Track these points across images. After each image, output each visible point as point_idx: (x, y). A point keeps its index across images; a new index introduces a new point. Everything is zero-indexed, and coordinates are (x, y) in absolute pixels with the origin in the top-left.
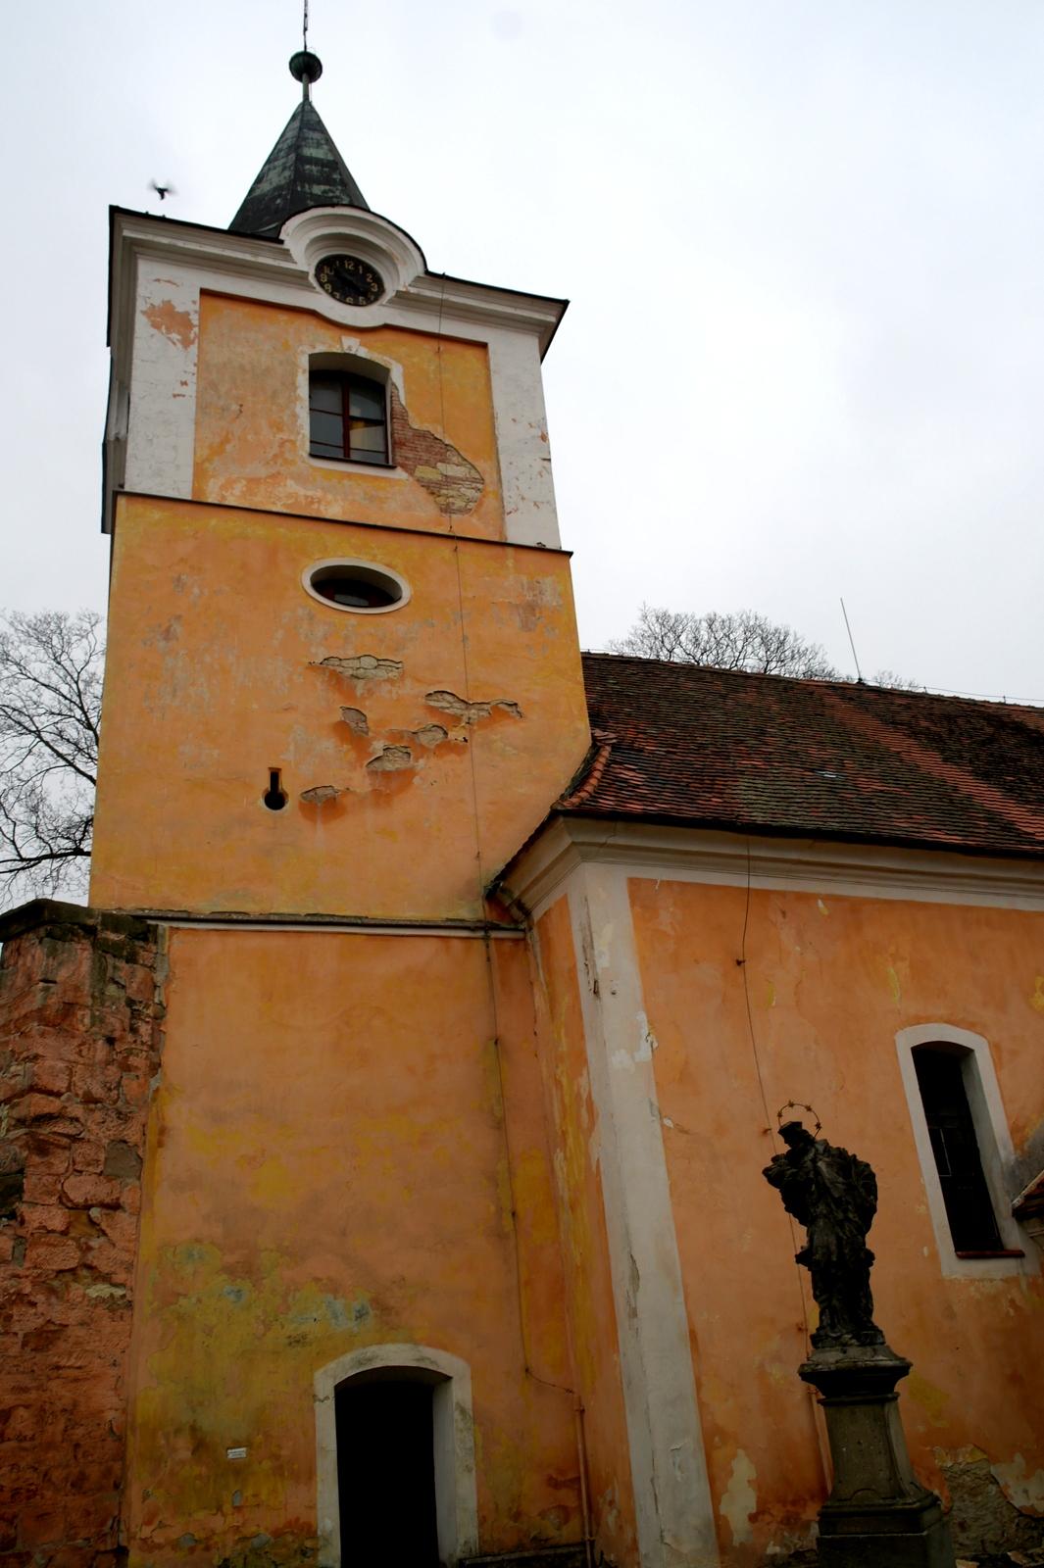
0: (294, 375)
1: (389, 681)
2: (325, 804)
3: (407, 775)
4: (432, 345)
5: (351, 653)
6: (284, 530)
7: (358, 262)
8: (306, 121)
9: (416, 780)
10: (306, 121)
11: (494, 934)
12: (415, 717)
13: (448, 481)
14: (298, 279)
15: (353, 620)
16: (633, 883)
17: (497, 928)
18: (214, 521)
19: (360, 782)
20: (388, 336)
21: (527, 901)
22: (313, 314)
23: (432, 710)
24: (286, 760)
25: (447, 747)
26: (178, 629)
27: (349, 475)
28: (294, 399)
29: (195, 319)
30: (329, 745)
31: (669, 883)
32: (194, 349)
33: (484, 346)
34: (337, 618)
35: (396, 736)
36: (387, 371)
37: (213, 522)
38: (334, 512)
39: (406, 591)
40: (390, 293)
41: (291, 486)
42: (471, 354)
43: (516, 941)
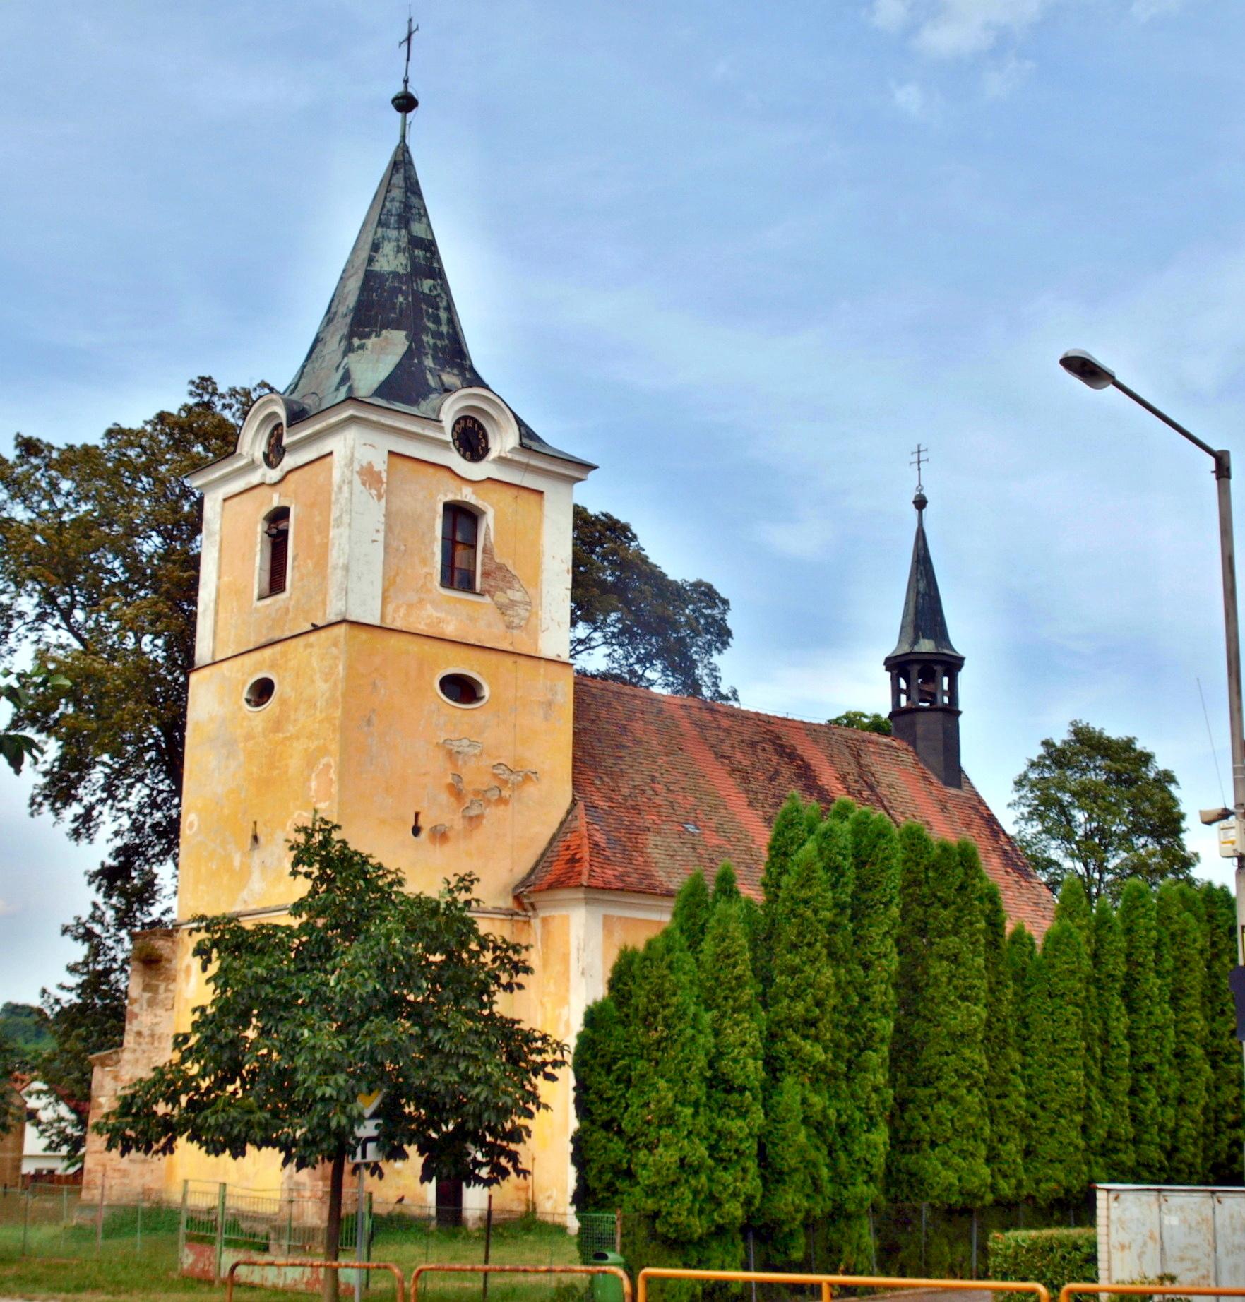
0: (434, 519)
1: (475, 755)
2: (440, 836)
3: (479, 817)
4: (513, 492)
5: (457, 736)
6: (429, 646)
7: (475, 421)
8: (402, 163)
9: (484, 821)
10: (402, 163)
11: (516, 918)
12: (485, 781)
13: (513, 603)
14: (444, 444)
15: (459, 713)
16: (606, 917)
17: (517, 914)
18: (394, 641)
19: (458, 824)
20: (489, 485)
21: (537, 905)
22: (449, 469)
23: (495, 776)
24: (423, 807)
25: (502, 801)
26: (374, 718)
27: (460, 600)
28: (433, 540)
29: (384, 475)
30: (444, 797)
31: (620, 918)
32: (384, 500)
33: (541, 493)
34: (451, 711)
35: (477, 792)
36: (484, 513)
37: (392, 641)
38: (450, 630)
39: (486, 692)
40: (493, 454)
41: (429, 610)
42: (533, 497)
43: (525, 922)
